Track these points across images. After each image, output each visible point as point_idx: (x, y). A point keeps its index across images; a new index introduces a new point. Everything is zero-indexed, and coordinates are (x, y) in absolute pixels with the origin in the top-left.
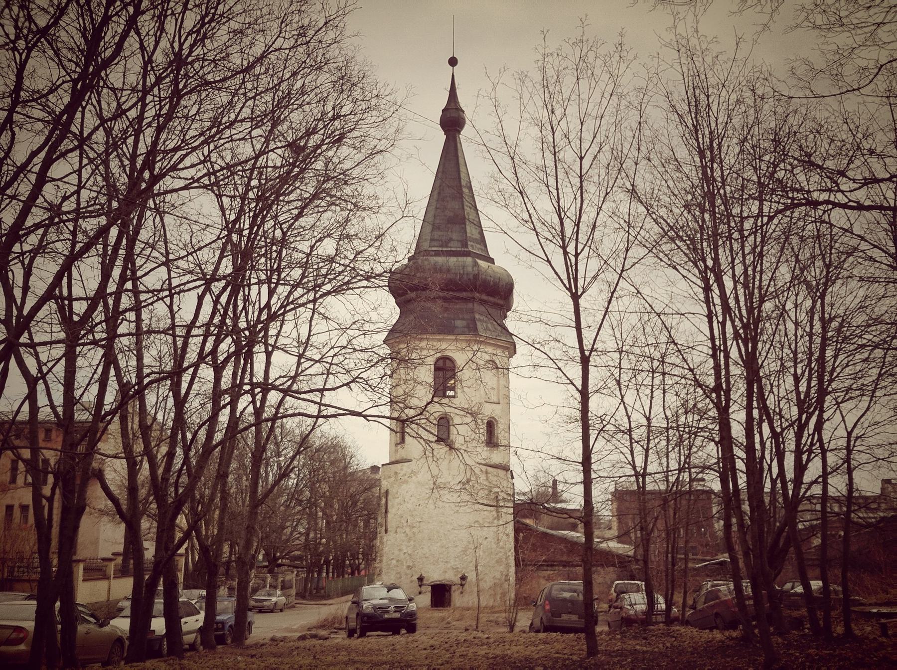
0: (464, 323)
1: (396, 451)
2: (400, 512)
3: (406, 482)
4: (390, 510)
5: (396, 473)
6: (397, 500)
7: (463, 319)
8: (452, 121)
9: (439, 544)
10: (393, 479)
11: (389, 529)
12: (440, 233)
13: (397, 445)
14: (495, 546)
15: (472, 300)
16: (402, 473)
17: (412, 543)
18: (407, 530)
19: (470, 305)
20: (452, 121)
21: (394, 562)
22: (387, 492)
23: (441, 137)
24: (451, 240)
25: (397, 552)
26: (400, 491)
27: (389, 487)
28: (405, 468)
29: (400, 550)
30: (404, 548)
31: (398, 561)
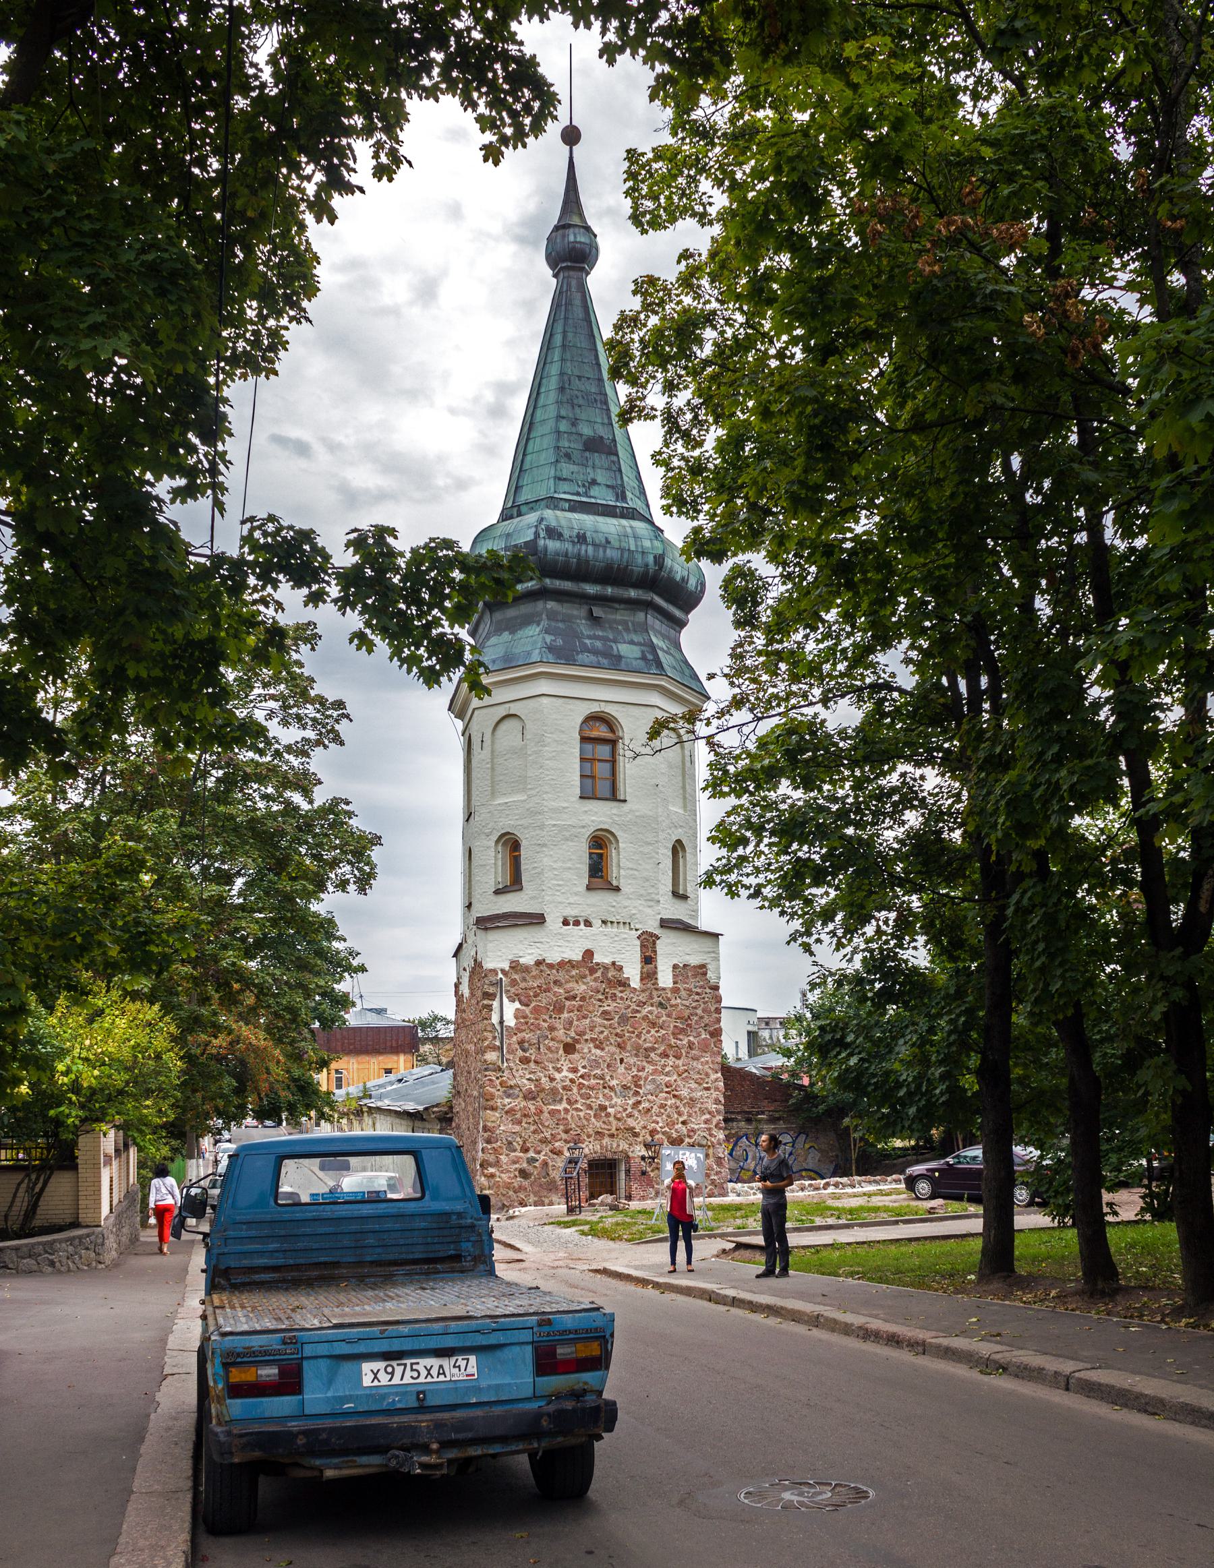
7: (632, 642)
15: (649, 606)
19: (641, 616)
24: (594, 482)
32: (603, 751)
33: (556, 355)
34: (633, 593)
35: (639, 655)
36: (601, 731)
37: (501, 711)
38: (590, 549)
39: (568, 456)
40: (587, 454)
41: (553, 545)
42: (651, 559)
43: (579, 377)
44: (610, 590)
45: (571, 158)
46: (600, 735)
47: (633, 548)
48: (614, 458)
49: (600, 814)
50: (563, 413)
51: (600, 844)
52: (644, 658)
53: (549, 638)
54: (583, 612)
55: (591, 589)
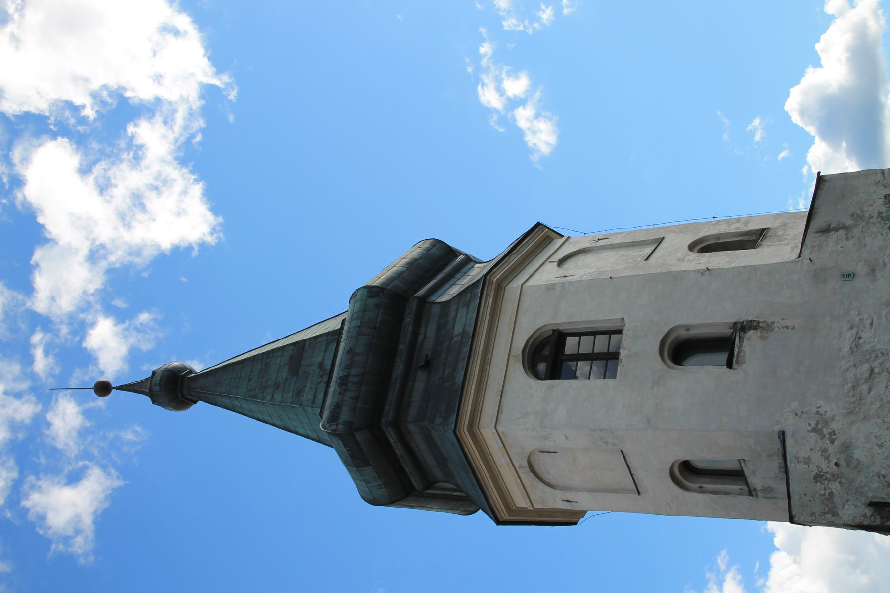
0: (462, 312)
1: (768, 490)
3: (847, 447)
5: (819, 477)
8: (174, 388)
12: (307, 389)
13: (751, 492)
15: (424, 301)
16: (817, 457)
19: (436, 310)
20: (174, 388)
23: (201, 411)
24: (321, 366)
27: (863, 499)
28: (804, 453)
32: (571, 346)
34: (409, 320)
35: (465, 310)
36: (547, 352)
37: (529, 479)
38: (354, 371)
39: (299, 393)
40: (300, 372)
41: (344, 416)
42: (372, 301)
43: (250, 380)
44: (403, 347)
45: (122, 388)
46: (550, 356)
47: (358, 323)
48: (307, 343)
49: (640, 350)
50: (269, 398)
51: (681, 349)
52: (468, 305)
53: (438, 420)
54: (421, 376)
55: (399, 368)
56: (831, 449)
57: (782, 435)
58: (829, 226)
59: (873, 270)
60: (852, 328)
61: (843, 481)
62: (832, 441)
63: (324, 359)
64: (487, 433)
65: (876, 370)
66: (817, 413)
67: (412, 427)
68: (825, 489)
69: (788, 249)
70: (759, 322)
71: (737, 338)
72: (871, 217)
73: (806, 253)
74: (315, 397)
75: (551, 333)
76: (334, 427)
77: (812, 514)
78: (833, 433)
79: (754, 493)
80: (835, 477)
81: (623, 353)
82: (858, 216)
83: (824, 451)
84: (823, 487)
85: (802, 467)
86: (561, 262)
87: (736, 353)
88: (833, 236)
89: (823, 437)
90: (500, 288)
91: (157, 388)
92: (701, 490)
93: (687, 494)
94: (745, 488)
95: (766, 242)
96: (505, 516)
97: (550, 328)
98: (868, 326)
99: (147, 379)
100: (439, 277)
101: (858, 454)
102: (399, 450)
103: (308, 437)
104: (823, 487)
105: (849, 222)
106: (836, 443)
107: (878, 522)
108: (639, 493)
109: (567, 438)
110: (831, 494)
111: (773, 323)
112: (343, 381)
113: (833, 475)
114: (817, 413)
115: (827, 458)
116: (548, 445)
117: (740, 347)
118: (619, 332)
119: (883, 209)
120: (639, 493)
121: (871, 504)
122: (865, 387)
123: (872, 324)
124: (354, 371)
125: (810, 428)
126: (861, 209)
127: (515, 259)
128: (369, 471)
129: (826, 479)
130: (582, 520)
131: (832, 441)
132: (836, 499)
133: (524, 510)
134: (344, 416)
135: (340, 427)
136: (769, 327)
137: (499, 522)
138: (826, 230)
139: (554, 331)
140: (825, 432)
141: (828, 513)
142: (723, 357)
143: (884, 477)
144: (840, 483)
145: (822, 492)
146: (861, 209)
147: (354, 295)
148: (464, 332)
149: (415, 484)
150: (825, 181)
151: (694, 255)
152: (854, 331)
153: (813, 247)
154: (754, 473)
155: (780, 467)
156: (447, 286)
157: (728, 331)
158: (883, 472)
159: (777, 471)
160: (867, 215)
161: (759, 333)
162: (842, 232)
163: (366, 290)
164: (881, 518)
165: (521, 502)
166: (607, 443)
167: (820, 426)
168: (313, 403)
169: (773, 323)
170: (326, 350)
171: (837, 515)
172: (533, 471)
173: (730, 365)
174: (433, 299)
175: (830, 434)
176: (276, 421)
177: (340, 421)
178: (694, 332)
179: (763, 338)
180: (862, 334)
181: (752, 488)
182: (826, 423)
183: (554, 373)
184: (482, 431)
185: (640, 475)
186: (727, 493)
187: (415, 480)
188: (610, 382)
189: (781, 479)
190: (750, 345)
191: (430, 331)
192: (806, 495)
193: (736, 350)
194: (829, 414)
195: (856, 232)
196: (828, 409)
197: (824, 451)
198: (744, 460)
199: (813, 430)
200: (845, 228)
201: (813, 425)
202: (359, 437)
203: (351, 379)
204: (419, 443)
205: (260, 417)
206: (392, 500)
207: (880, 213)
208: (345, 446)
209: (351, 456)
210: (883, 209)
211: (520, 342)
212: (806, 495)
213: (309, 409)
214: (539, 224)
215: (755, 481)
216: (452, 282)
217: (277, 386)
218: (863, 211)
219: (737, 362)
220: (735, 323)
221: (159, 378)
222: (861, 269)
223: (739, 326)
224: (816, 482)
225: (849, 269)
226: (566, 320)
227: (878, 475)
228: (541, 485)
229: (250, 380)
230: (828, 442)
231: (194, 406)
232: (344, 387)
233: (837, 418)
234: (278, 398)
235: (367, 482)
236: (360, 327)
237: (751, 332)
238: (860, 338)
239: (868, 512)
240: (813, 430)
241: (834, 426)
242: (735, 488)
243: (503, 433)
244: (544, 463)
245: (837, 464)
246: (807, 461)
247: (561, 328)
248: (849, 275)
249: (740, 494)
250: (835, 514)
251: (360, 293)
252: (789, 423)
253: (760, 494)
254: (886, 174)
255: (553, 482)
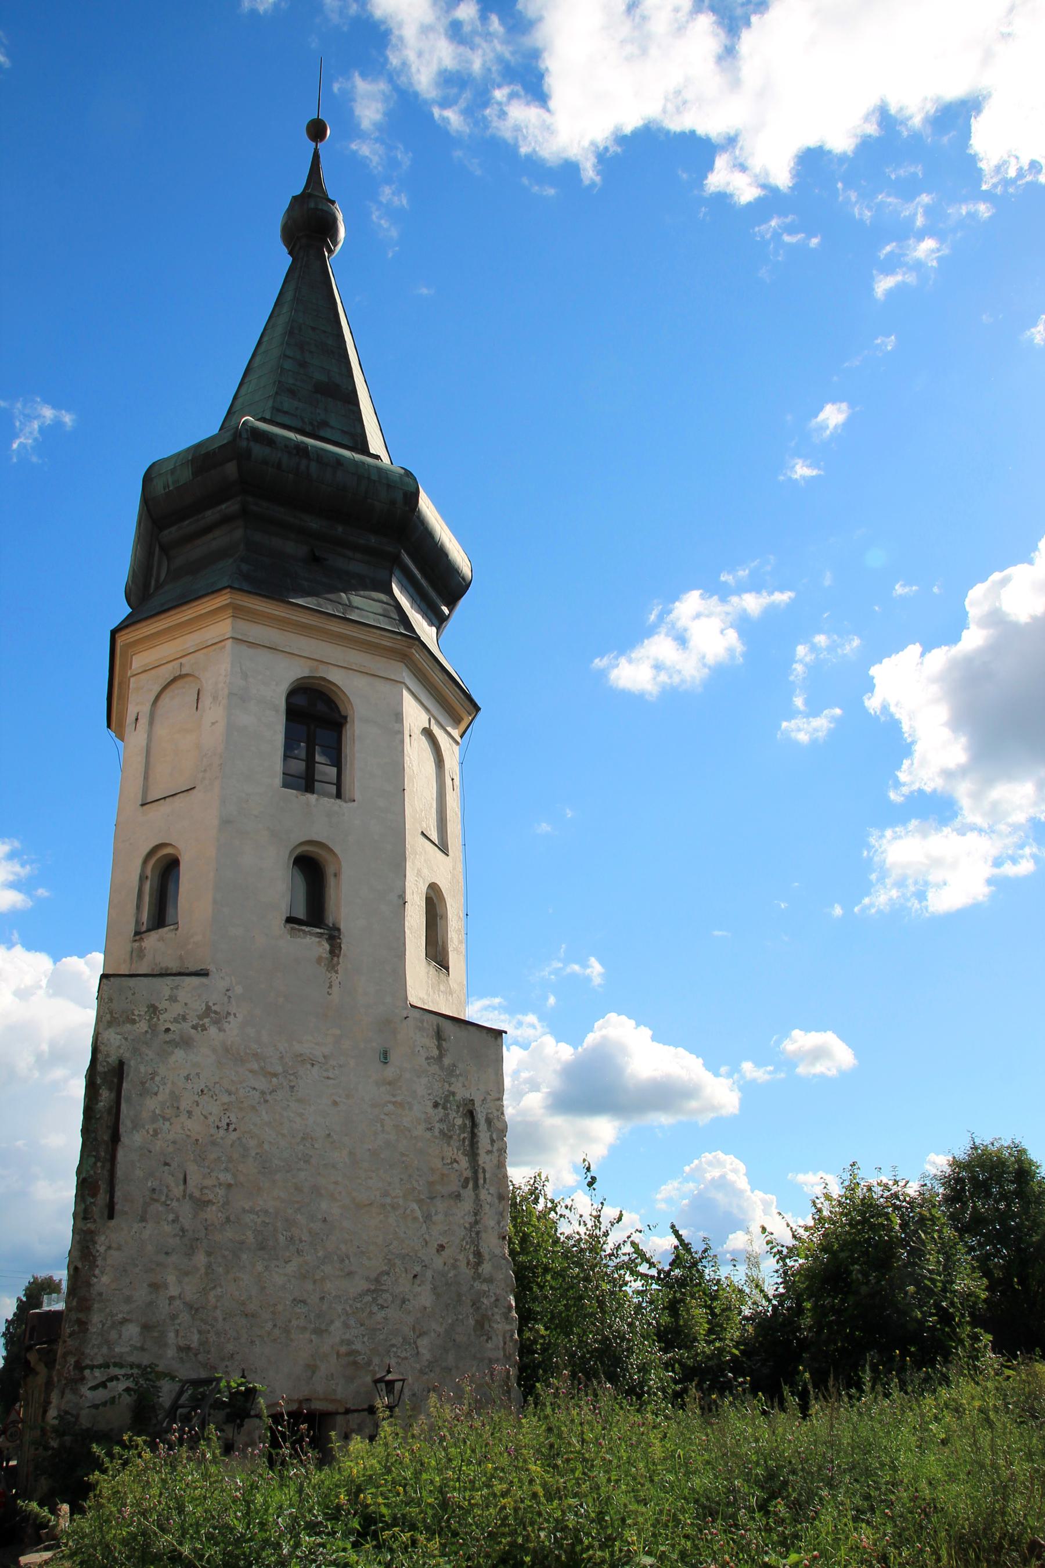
0: (377, 607)
1: (141, 953)
2: (158, 1145)
3: (185, 1043)
4: (125, 1139)
5: (153, 1010)
6: (152, 1104)
9: (291, 1268)
10: (143, 1026)
11: (117, 1207)
14: (467, 1272)
15: (395, 561)
16: (177, 1009)
17: (200, 1259)
18: (186, 1210)
21: (132, 1331)
22: (119, 1070)
23: (280, 260)
24: (324, 424)
25: (141, 1294)
26: (162, 1071)
27: (127, 1055)
28: (182, 995)
29: (155, 1287)
30: (171, 1279)
31: (146, 1328)
33: (285, 309)
34: (373, 540)
36: (321, 707)
37: (167, 672)
38: (313, 466)
39: (292, 393)
41: (258, 450)
42: (399, 497)
43: (314, 329)
45: (316, 157)
47: (374, 477)
49: (314, 818)
50: (289, 353)
51: (311, 868)
53: (245, 567)
55: (314, 524)
56: (186, 1026)
57: (203, 973)
58: (445, 1040)
59: (390, 1083)
60: (324, 1057)
61: (149, 1036)
62: (195, 1027)
63: (332, 428)
64: (224, 627)
65: (274, 1080)
66: (229, 1014)
67: (239, 534)
68: (139, 1015)
69: (423, 994)
70: (338, 957)
71: (319, 930)
72: (450, 1084)
73: (416, 1014)
74: (286, 413)
75: (343, 713)
76: (244, 436)
77: (111, 1000)
78: (204, 1029)
79: (137, 938)
80: (153, 1028)
81: (312, 798)
82: (453, 1071)
83: (184, 1018)
84: (142, 1013)
85: (167, 992)
86: (428, 733)
87: (304, 928)
88: (432, 1043)
89: (200, 1017)
90: (404, 658)
91: (312, 205)
92: (142, 878)
93: (139, 862)
94: (144, 928)
95: (432, 971)
96: (121, 640)
97: (350, 713)
98: (325, 1074)
99: (324, 193)
100: (423, 582)
101: (179, 1054)
102: (211, 515)
103: (235, 398)
104: (142, 1013)
105: (447, 1061)
106: (193, 1031)
107: (100, 1068)
108: (142, 805)
109: (213, 724)
110: (134, 1022)
111: (337, 972)
112: (301, 450)
113: (156, 1025)
114: (229, 1014)
115: (176, 1020)
116: (206, 701)
117: (311, 934)
118: (339, 795)
119: (458, 1097)
120: (142, 805)
121: (121, 1064)
122: (256, 1067)
123: (328, 1078)
124: (314, 466)
125: (211, 1004)
126: (461, 1075)
127: (437, 678)
128: (186, 475)
129: (151, 1018)
130: (113, 735)
131: (195, 1027)
132: (128, 1027)
133: (127, 664)
134: (258, 450)
135: (244, 444)
136: (332, 967)
137: (114, 633)
138: (439, 1035)
139: (345, 718)
140: (206, 1020)
141: (112, 1016)
142: (301, 913)
143: (152, 1079)
144: (146, 1032)
145: (136, 1013)
146: (461, 1075)
147: (408, 474)
148: (351, 606)
149: (166, 532)
150: (496, 1038)
151: (424, 889)
152: (321, 1059)
153: (422, 1021)
154: (161, 939)
155: (167, 968)
156: (411, 590)
157: (330, 921)
158: (157, 1079)
159: (163, 965)
160: (453, 1080)
161: (326, 955)
162: (435, 1052)
163: (413, 490)
164: (105, 1073)
165: (138, 662)
166: (205, 771)
167: (213, 1015)
168: (278, 410)
169: (337, 972)
170: (343, 432)
171: (109, 1027)
172: (175, 680)
173: (290, 920)
174: (397, 572)
175: (203, 1025)
176: (258, 359)
177: (252, 444)
178: (331, 882)
179: (319, 960)
180: (316, 1068)
181: (143, 936)
182: (216, 1022)
183: (294, 714)
184: (229, 621)
185: (164, 809)
186: (139, 907)
187: (170, 534)
188: (278, 780)
189: (153, 969)
190: (311, 945)
191: (356, 567)
192: (133, 994)
193: (307, 929)
194: (226, 1026)
195: (434, 1068)
196: (232, 1027)
197: (184, 1018)
198: (177, 929)
199: (208, 1008)
200: (441, 1056)
201: (214, 1008)
202: (231, 469)
203: (304, 462)
204: (218, 540)
205: (265, 339)
206: (147, 500)
207: (454, 1094)
208: (220, 447)
209: (207, 455)
210: (458, 1097)
211: (335, 676)
212: (133, 994)
213: (270, 403)
214: (477, 709)
215: (152, 940)
216: (416, 597)
217: (303, 364)
218: (458, 1076)
219: (292, 929)
220: (339, 930)
221: (325, 208)
222: (390, 1072)
223: (336, 933)
224: (148, 1007)
225: (393, 1057)
226: (357, 732)
227: (154, 1074)
228: (157, 689)
229: (314, 329)
230: (194, 1022)
231: (286, 251)
232: (295, 452)
233: (221, 1034)
234: (288, 365)
235: (173, 471)
236: (369, 478)
237: (327, 947)
238: (313, 1065)
239: (113, 1059)
240: (208, 1008)
241: (213, 1030)
242: (145, 917)
243: (224, 647)
244: (183, 695)
245: (168, 1030)
246: (173, 999)
247: (348, 726)
248: (386, 1058)
249: (137, 922)
250: (110, 1024)
251: (411, 481)
252: (218, 983)
253: (137, 944)
254: (497, 1103)
255: (160, 703)
